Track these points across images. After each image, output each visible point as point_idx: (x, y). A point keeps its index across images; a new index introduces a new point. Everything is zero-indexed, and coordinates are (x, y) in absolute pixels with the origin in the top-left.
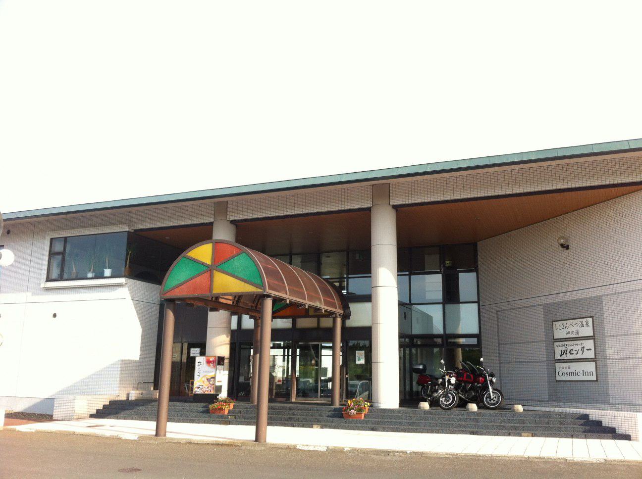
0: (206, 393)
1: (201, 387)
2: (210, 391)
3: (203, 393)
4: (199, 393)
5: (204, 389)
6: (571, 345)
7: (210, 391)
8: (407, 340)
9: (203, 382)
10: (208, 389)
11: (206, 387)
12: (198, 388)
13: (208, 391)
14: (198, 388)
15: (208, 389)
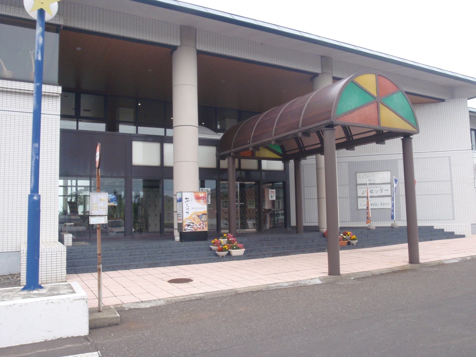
0: (198, 230)
1: (191, 224)
2: (203, 228)
3: (193, 230)
4: (189, 231)
5: (195, 227)
6: (370, 188)
7: (203, 228)
8: (243, 173)
9: (194, 219)
10: (200, 226)
11: (198, 225)
12: (188, 225)
13: (200, 228)
14: (188, 225)
15: (200, 226)
